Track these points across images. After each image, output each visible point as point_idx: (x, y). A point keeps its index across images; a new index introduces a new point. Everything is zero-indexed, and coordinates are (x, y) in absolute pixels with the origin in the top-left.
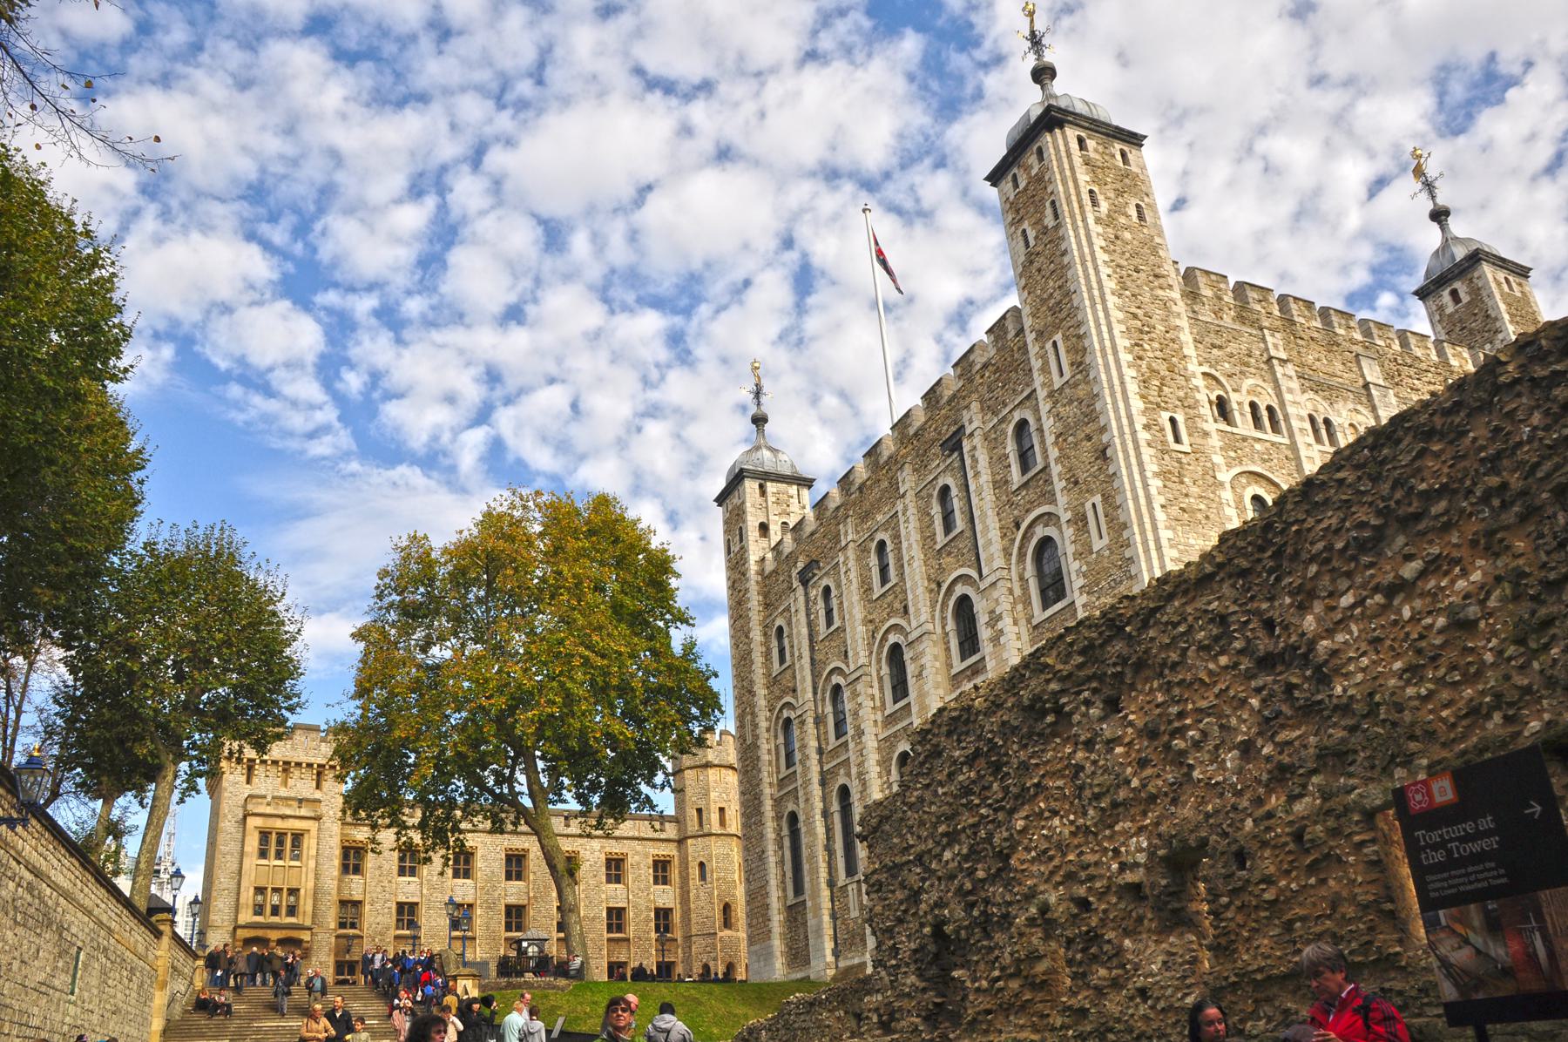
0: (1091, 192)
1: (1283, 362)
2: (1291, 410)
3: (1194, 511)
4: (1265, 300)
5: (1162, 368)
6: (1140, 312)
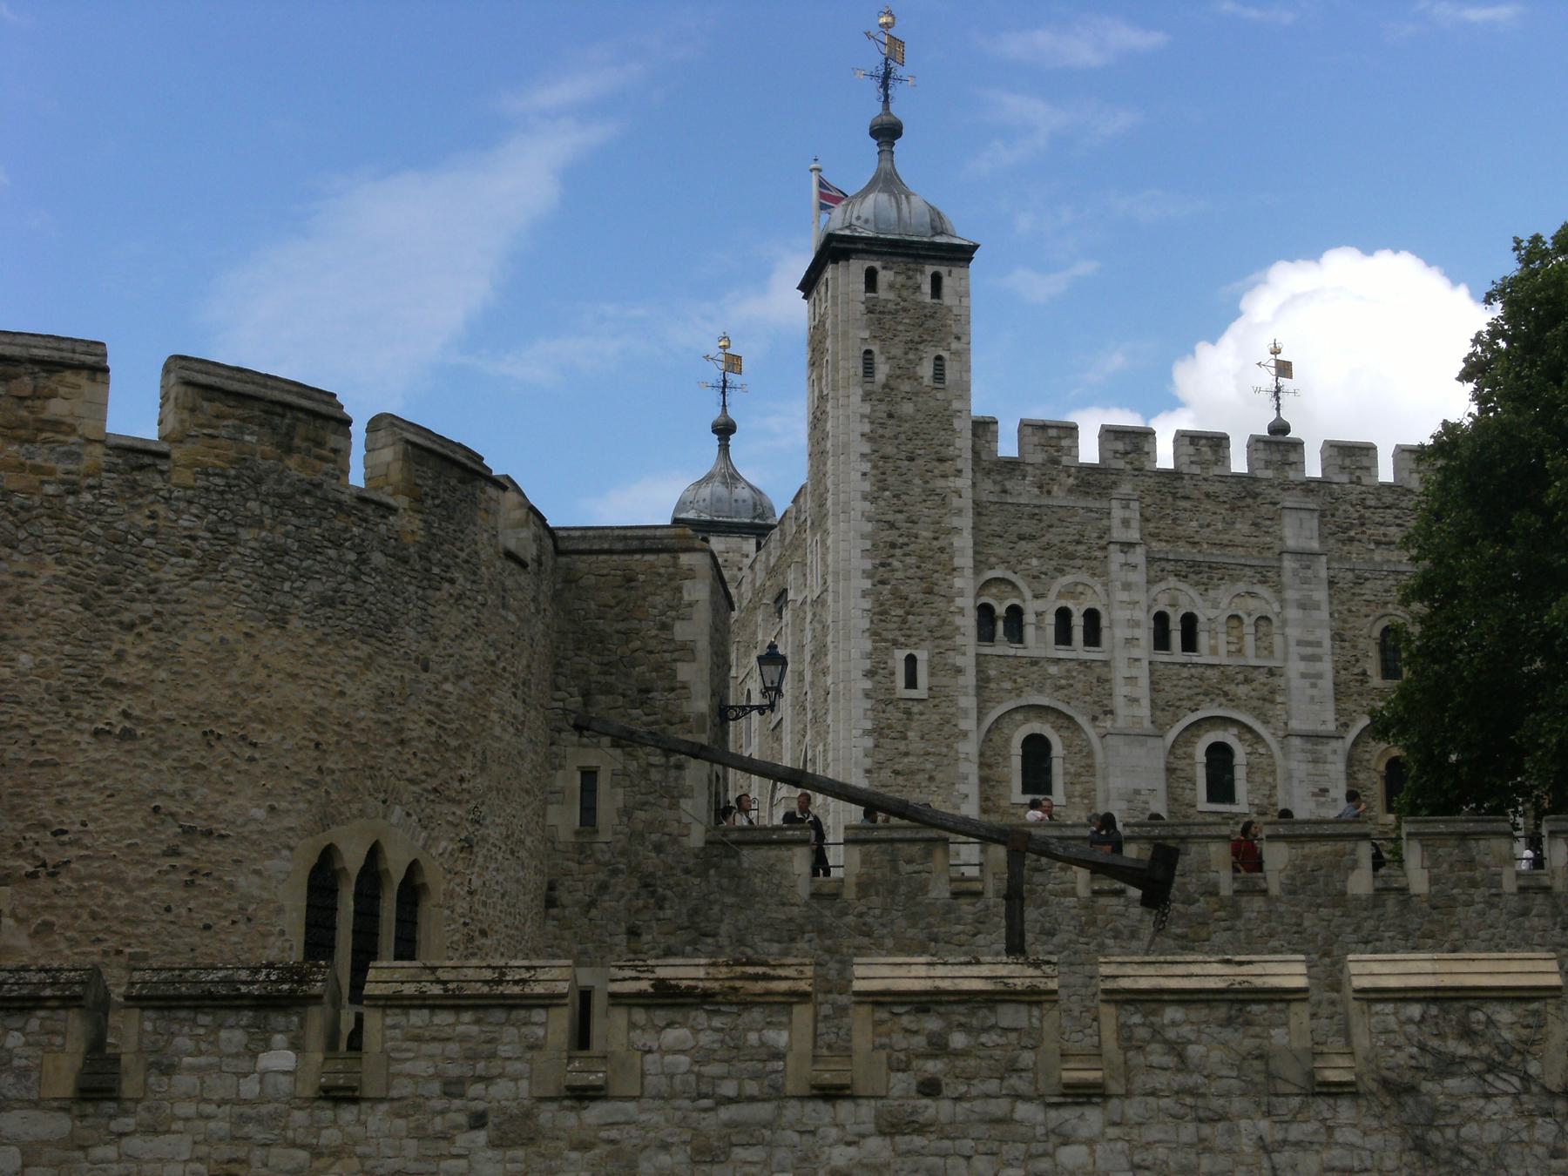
1: (1127, 546)
2: (1121, 614)
3: (913, 773)
4: (1138, 449)
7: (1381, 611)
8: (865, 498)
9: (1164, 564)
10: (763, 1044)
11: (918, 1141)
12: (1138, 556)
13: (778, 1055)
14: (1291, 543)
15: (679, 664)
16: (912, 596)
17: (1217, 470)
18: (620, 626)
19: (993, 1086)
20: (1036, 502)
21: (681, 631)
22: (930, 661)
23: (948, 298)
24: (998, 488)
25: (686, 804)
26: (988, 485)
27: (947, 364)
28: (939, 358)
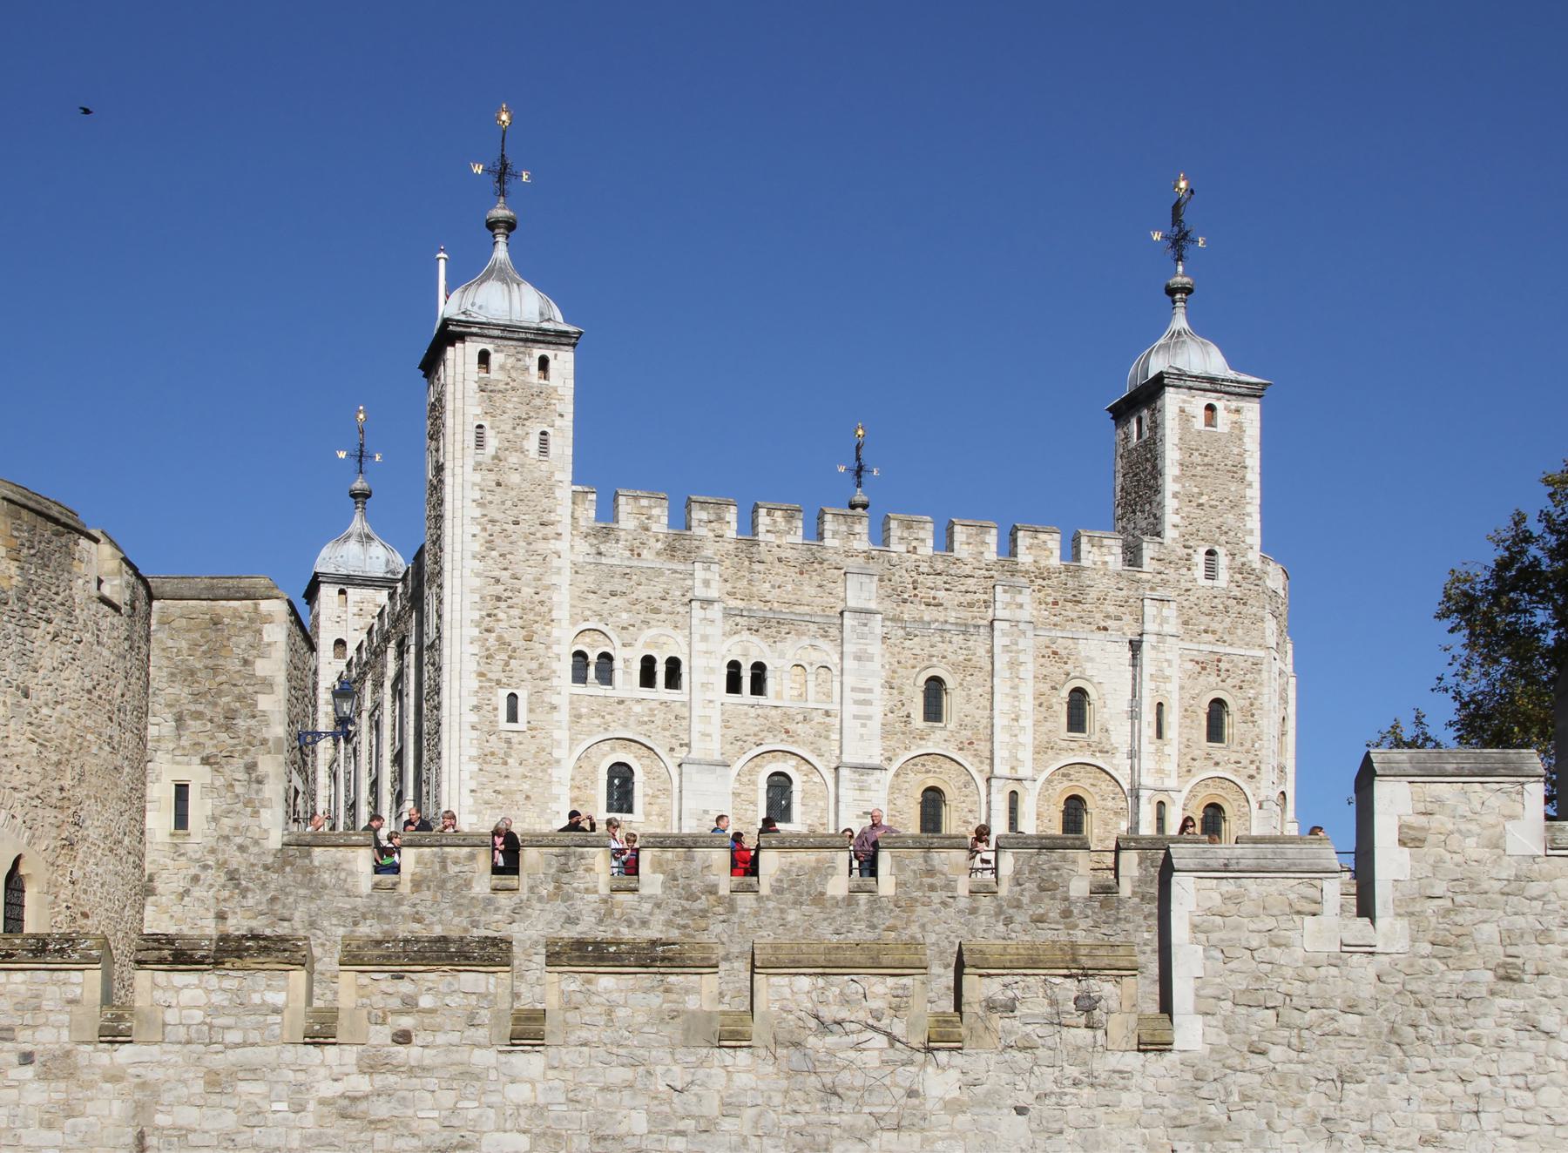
4: (720, 519)
5: (516, 638)
6: (505, 575)
7: (927, 663)
9: (738, 619)
10: (264, 1003)
11: (392, 1079)
12: (716, 611)
13: (277, 1011)
14: (852, 603)
15: (260, 696)
17: (790, 539)
18: (210, 663)
19: (455, 1037)
20: (627, 563)
21: (262, 668)
24: (593, 551)
25: (265, 814)
26: (583, 547)
28: (544, 433)
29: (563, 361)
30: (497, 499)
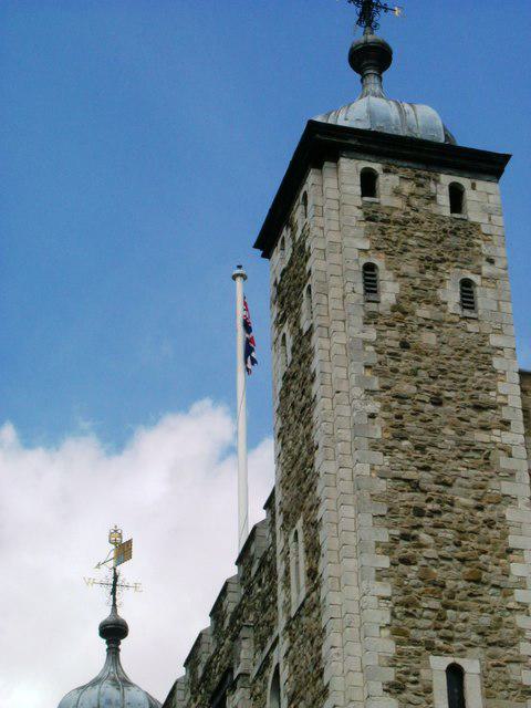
0: (369, 269)
5: (454, 577)
8: (375, 448)
16: (450, 584)
22: (483, 675)
23: (473, 212)
27: (478, 291)
29: (481, 196)
30: (403, 366)
